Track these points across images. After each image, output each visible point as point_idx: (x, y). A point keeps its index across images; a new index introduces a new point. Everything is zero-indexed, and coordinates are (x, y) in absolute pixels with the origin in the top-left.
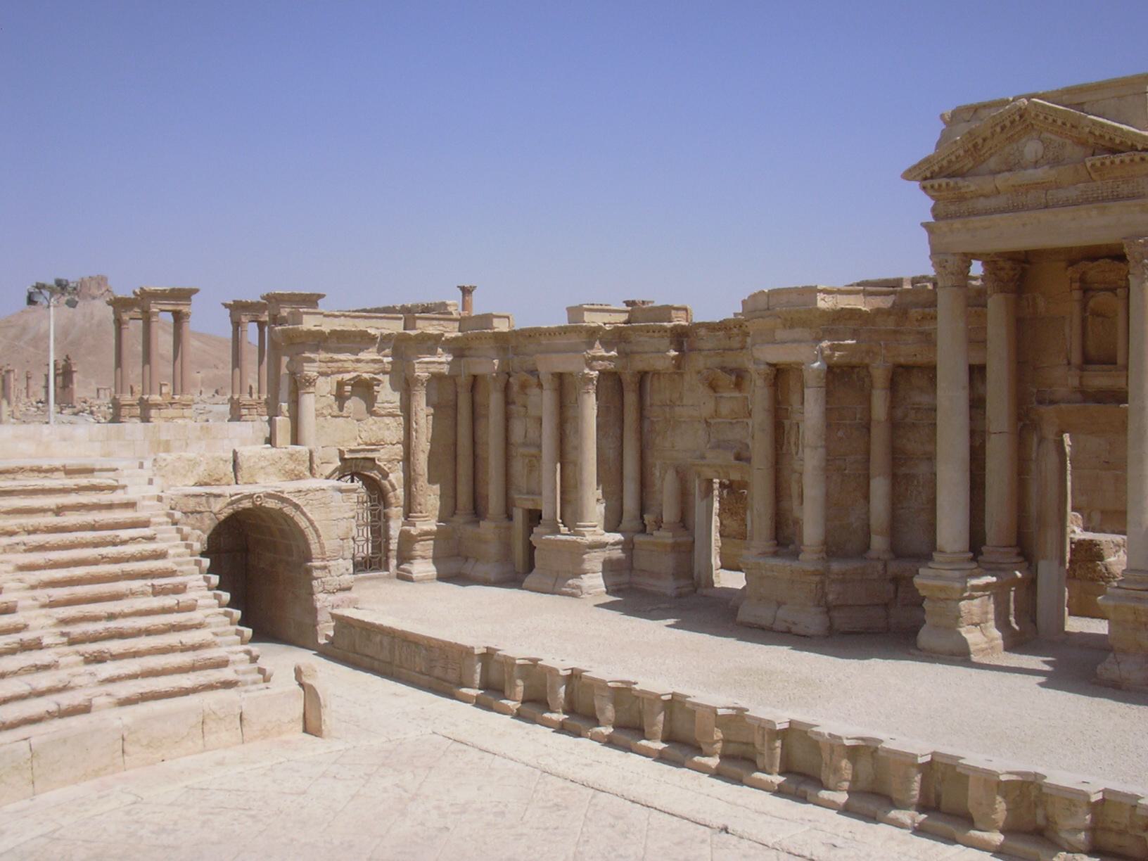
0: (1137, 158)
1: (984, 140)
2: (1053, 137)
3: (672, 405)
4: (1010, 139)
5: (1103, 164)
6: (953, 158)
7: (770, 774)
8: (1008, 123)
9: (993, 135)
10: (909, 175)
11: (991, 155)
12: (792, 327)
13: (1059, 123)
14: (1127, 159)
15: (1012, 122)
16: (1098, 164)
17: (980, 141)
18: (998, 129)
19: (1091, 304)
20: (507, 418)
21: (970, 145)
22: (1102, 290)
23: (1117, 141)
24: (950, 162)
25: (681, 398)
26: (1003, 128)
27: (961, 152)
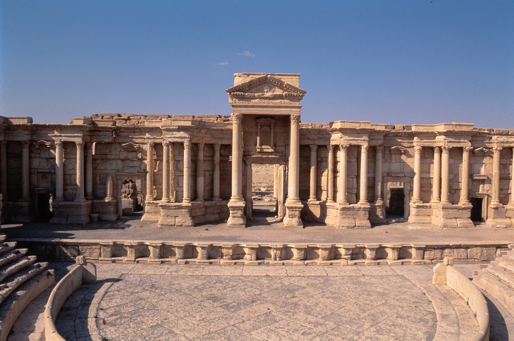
3: (106, 155)
4: (259, 85)
10: (228, 91)
20: (30, 157)
25: (111, 152)
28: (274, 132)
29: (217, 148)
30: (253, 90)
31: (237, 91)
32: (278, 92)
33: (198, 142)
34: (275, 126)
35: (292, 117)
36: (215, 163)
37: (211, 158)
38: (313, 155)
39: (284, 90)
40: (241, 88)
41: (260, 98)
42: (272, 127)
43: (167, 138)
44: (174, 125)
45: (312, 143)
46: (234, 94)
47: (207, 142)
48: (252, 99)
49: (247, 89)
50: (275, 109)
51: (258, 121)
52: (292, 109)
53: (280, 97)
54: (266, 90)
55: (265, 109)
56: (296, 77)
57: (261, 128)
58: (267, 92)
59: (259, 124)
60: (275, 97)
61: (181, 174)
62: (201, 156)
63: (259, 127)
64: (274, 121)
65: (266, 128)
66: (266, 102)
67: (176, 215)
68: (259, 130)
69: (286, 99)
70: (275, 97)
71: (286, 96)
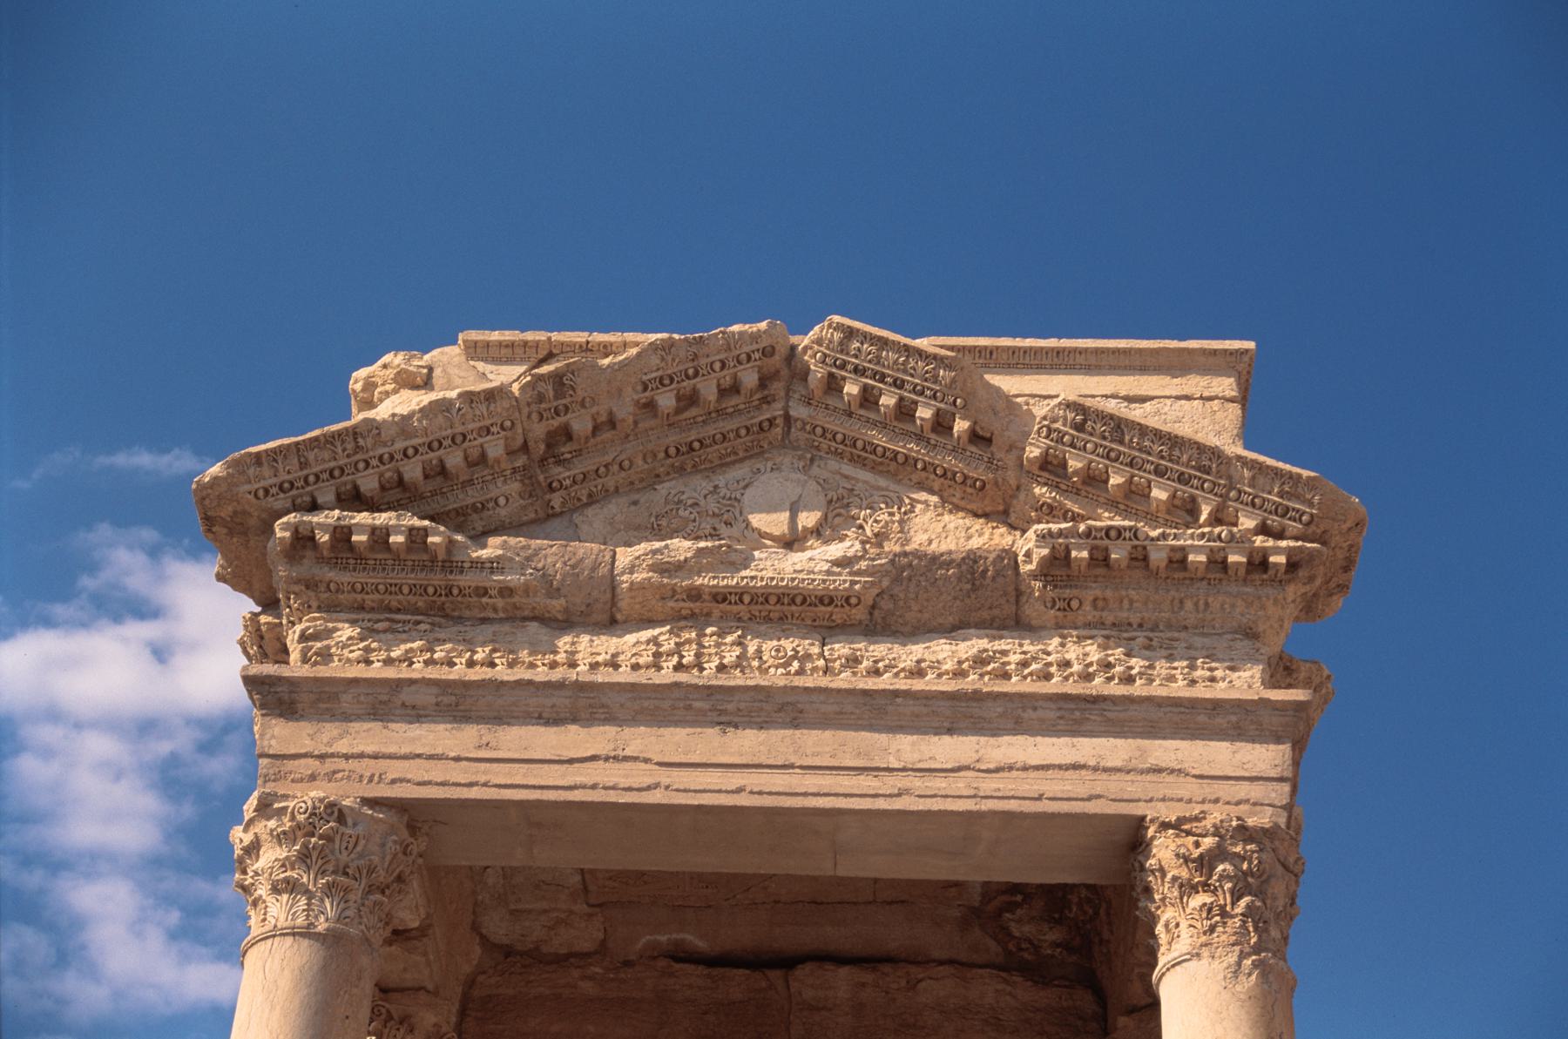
6: (454, 460)
8: (708, 390)
18: (666, 401)
21: (539, 430)
26: (690, 399)
30: (596, 517)
31: (354, 500)
32: (940, 530)
35: (1164, 851)
40: (437, 473)
41: (693, 608)
46: (303, 540)
48: (566, 623)
49: (508, 493)
50: (906, 748)
52: (1167, 751)
53: (981, 598)
54: (773, 522)
55: (747, 742)
56: (1195, 384)
58: (791, 542)
60: (900, 600)
66: (774, 659)
69: (1066, 621)
70: (900, 600)
71: (1057, 566)
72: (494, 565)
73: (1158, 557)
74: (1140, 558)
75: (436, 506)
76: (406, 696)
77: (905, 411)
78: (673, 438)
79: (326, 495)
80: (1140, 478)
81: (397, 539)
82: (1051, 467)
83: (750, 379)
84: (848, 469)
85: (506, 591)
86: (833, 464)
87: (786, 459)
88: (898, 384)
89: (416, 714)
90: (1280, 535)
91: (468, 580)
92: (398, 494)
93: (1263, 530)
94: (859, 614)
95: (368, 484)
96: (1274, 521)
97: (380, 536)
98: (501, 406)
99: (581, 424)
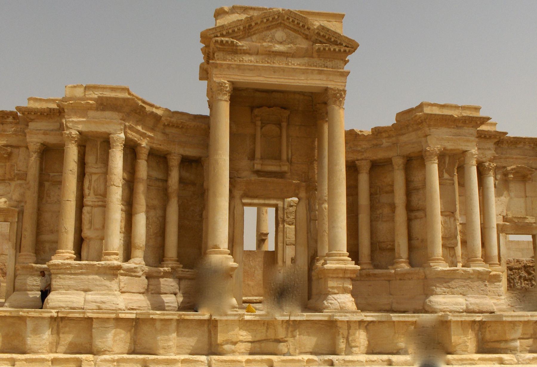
0: (342, 50)
1: (256, 24)
2: (291, 32)
4: (268, 28)
5: (324, 49)
6: (236, 30)
7: (295, 355)
8: (271, 19)
9: (262, 22)
11: (254, 34)
12: (103, 110)
13: (301, 25)
14: (337, 50)
15: (273, 18)
16: (322, 49)
17: (253, 24)
18: (265, 20)
19: (263, 129)
21: (247, 25)
22: (268, 124)
23: (332, 40)
24: (233, 31)
27: (242, 28)
28: (288, 136)
29: (174, 162)
30: (254, 38)
31: (222, 35)
33: (139, 142)
34: (288, 125)
36: (170, 190)
37: (161, 184)
38: (364, 179)
39: (315, 42)
42: (284, 124)
43: (75, 125)
44: (90, 96)
45: (359, 158)
47: (154, 146)
51: (256, 111)
57: (261, 128)
59: (260, 118)
61: (100, 203)
62: (143, 169)
63: (259, 123)
64: (287, 113)
65: (272, 128)
67: (86, 287)
68: (259, 129)
72: (242, 46)
73: (332, 49)
74: (330, 49)
75: (233, 35)
76: (232, 66)
77: (298, 24)
78: (266, 25)
79: (219, 35)
80: (330, 37)
81: (230, 42)
82: (318, 34)
83: (276, 17)
84: (289, 31)
85: (244, 50)
86: (287, 30)
87: (280, 29)
88: (298, 20)
89: (233, 68)
90: (348, 47)
91: (239, 48)
92: (228, 35)
93: (346, 46)
94: (291, 55)
95: (224, 33)
96: (347, 45)
97: (227, 42)
98: (243, 22)
99: (253, 24)
